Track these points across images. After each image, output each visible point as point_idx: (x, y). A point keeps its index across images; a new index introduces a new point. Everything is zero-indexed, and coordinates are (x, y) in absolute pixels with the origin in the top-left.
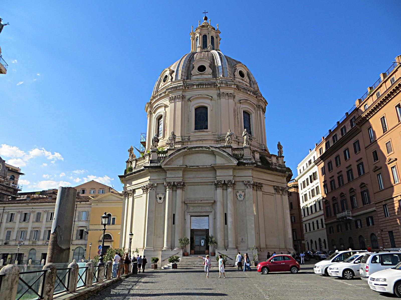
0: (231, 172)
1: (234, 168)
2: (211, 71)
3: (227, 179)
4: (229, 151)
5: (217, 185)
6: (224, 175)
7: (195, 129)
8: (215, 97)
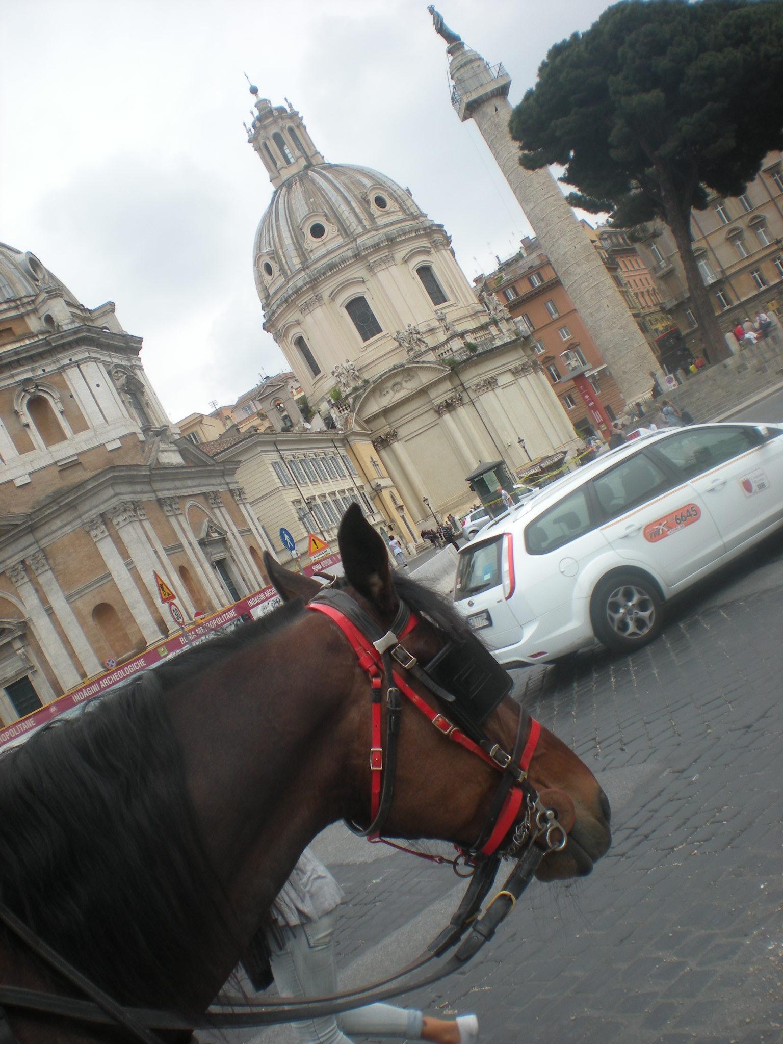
0: (447, 385)
1: (450, 377)
4: (431, 357)
5: (439, 411)
6: (441, 394)
7: (365, 338)
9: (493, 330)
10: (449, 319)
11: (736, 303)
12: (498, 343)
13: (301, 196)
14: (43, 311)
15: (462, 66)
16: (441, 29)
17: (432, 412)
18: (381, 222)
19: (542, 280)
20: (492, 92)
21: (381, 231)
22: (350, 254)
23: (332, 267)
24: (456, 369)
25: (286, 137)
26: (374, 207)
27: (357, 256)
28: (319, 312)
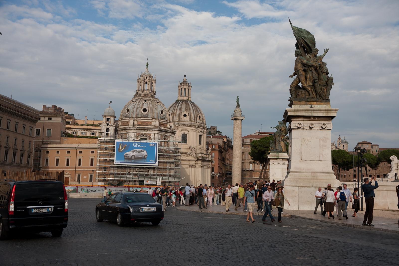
0: (194, 162)
2: (189, 117)
4: (194, 154)
5: (190, 166)
6: (193, 163)
9: (208, 156)
10: (202, 149)
11: (253, 177)
12: (207, 159)
13: (185, 106)
14: (171, 125)
15: (237, 111)
16: (237, 102)
17: (188, 165)
18: (198, 121)
19: (215, 148)
20: (240, 119)
21: (197, 123)
22: (189, 124)
23: (184, 125)
24: (198, 160)
25: (187, 90)
26: (198, 117)
27: (190, 126)
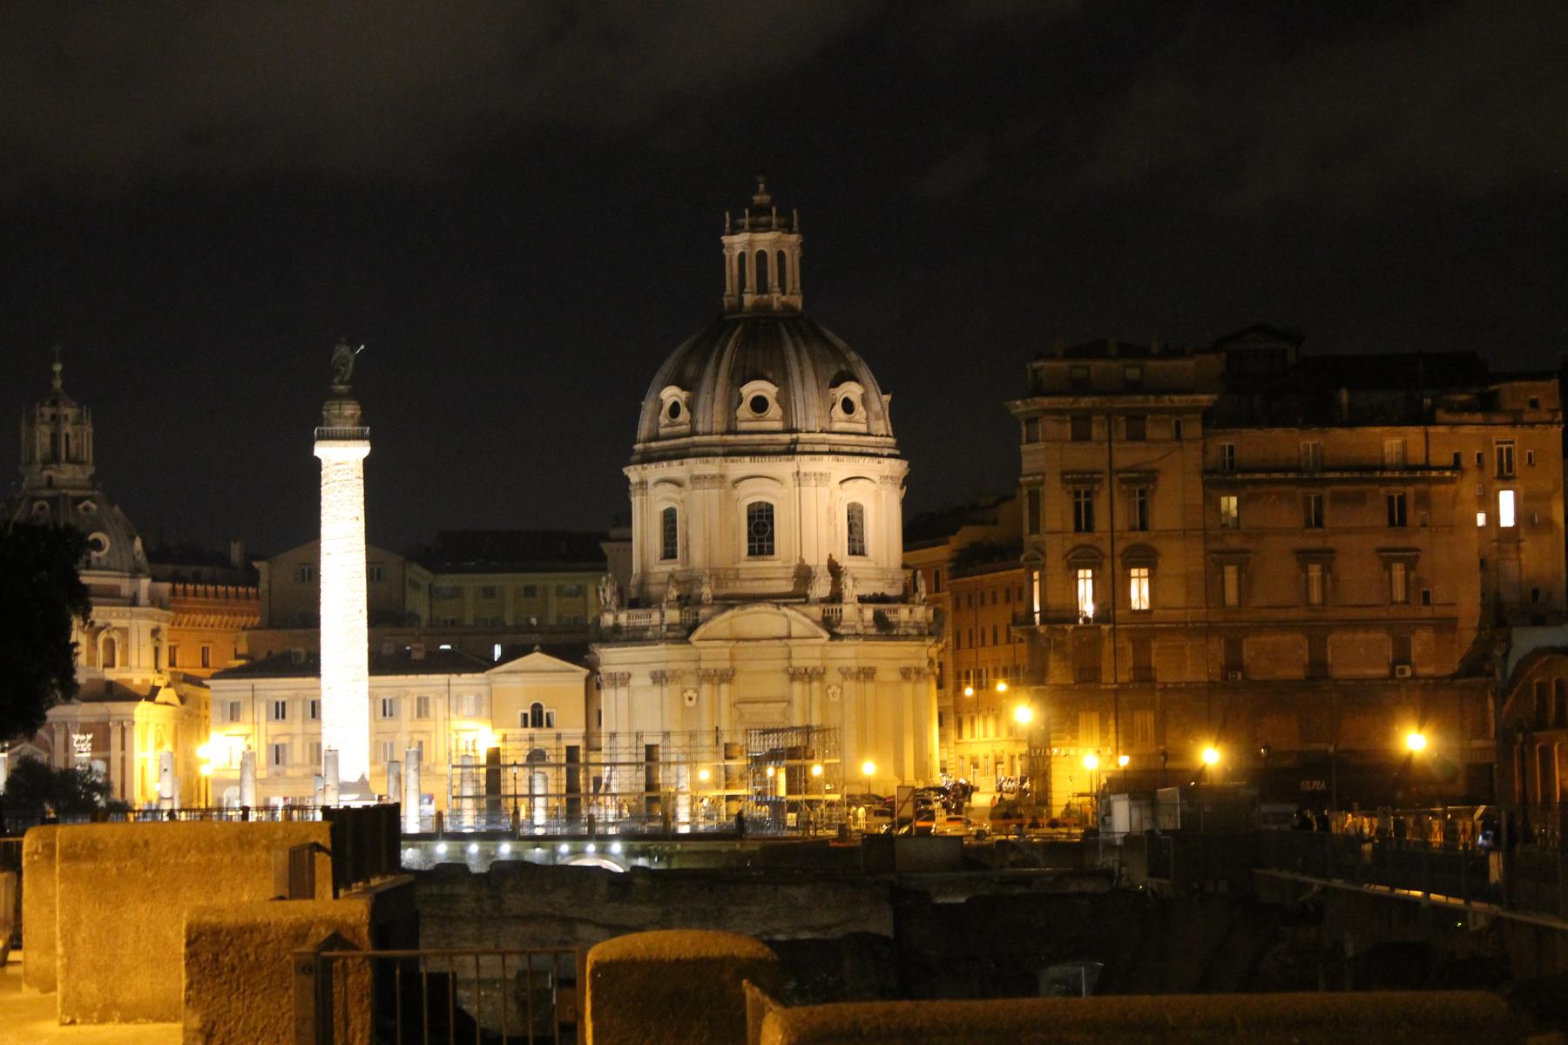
3: (810, 664)
5: (794, 676)
6: (807, 655)
8: (790, 481)
28: (714, 493)
